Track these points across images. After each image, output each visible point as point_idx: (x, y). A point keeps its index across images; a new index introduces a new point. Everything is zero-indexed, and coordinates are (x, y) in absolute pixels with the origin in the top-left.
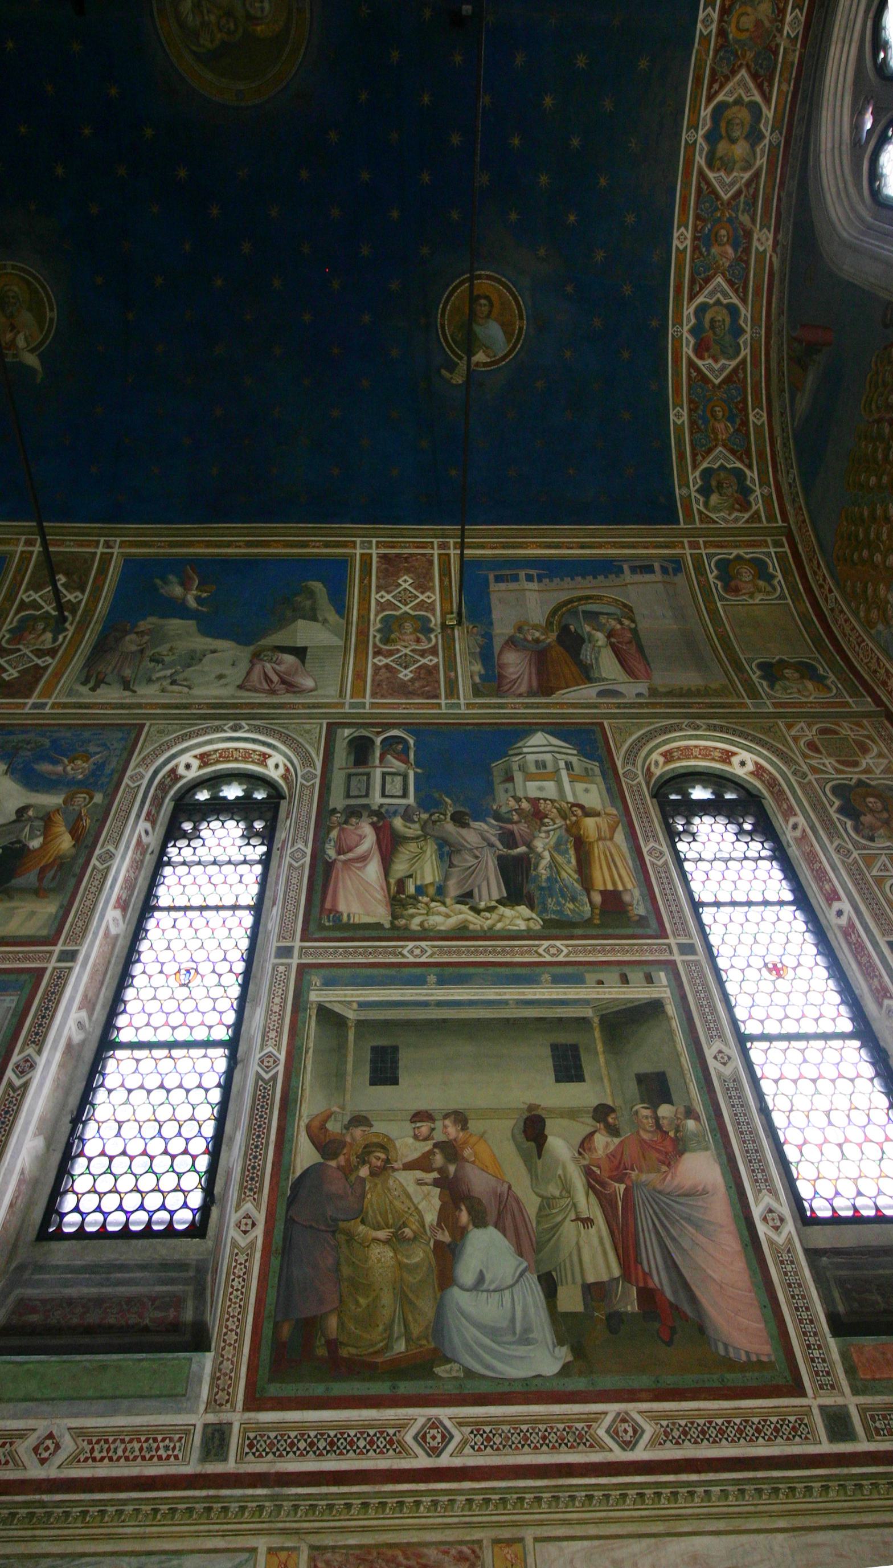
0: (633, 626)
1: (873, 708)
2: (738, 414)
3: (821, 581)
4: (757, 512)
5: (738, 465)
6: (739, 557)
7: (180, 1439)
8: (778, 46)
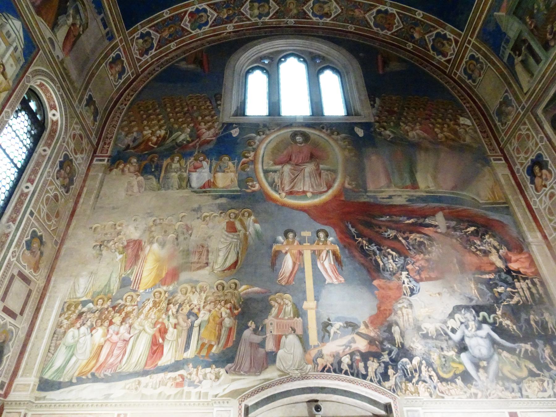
0: (81, 33)
1: (95, 143)
2: (173, 37)
3: (127, 99)
4: (141, 60)
5: (155, 45)
6: (123, 62)
8: (285, 18)
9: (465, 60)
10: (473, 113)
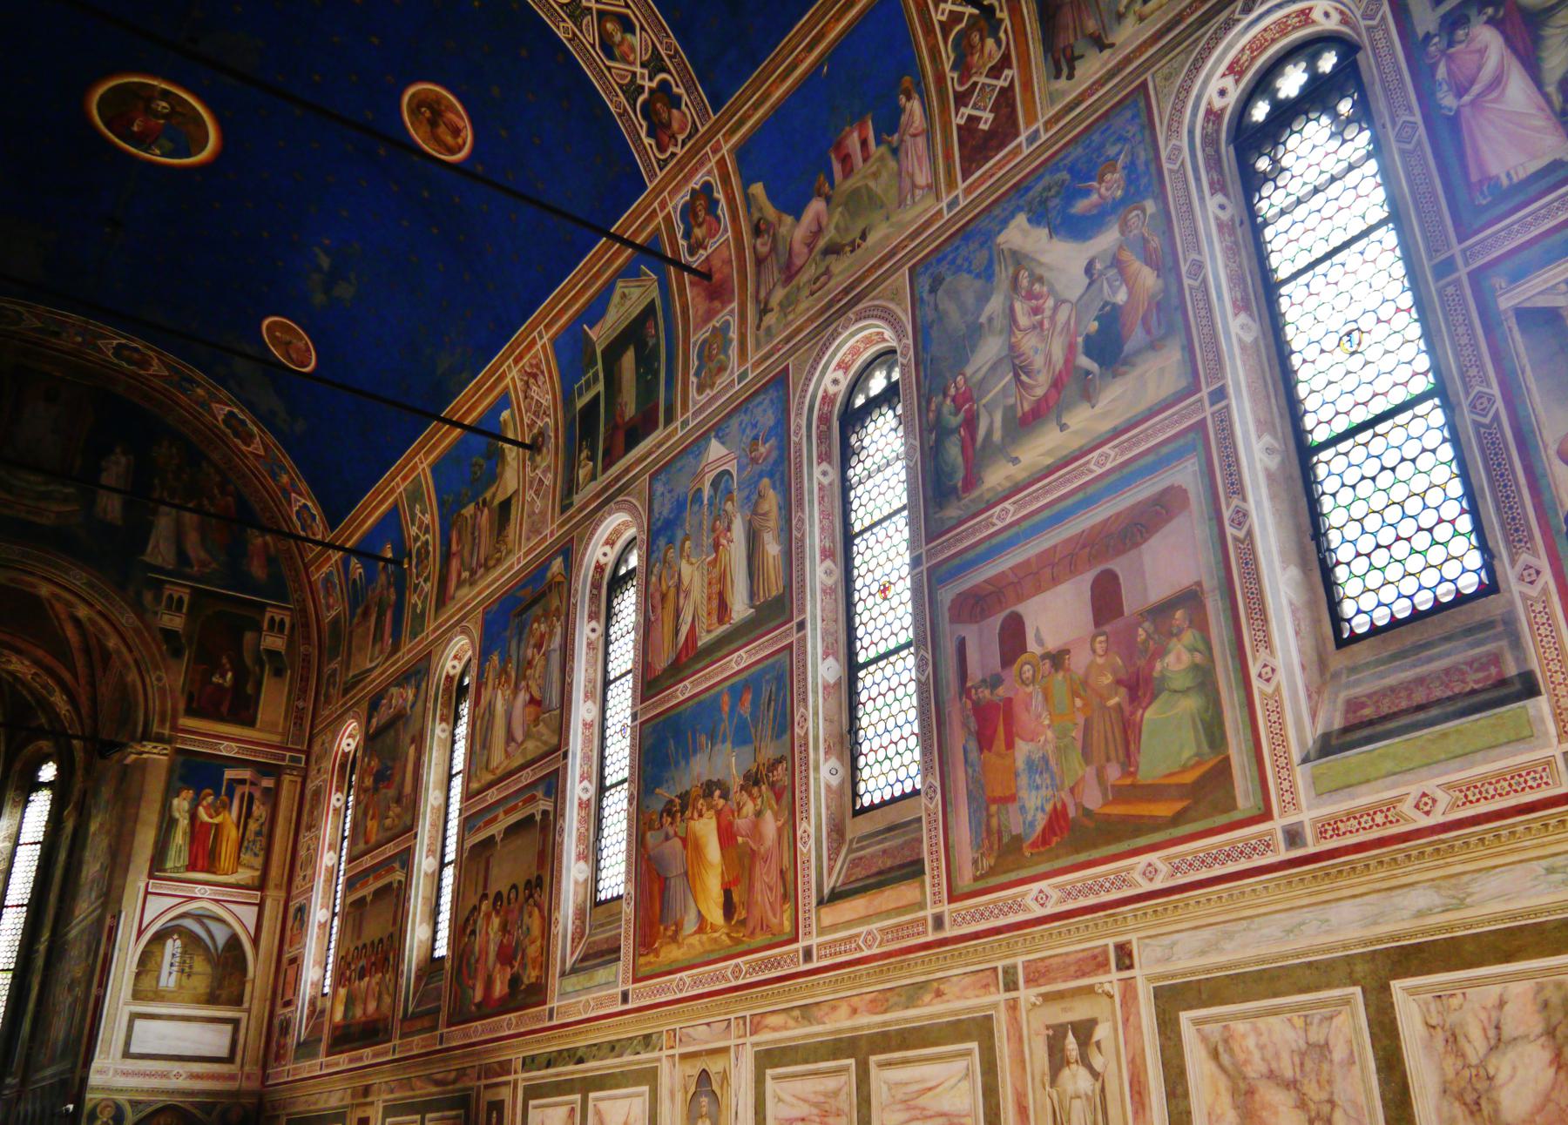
7: (1544, 769)
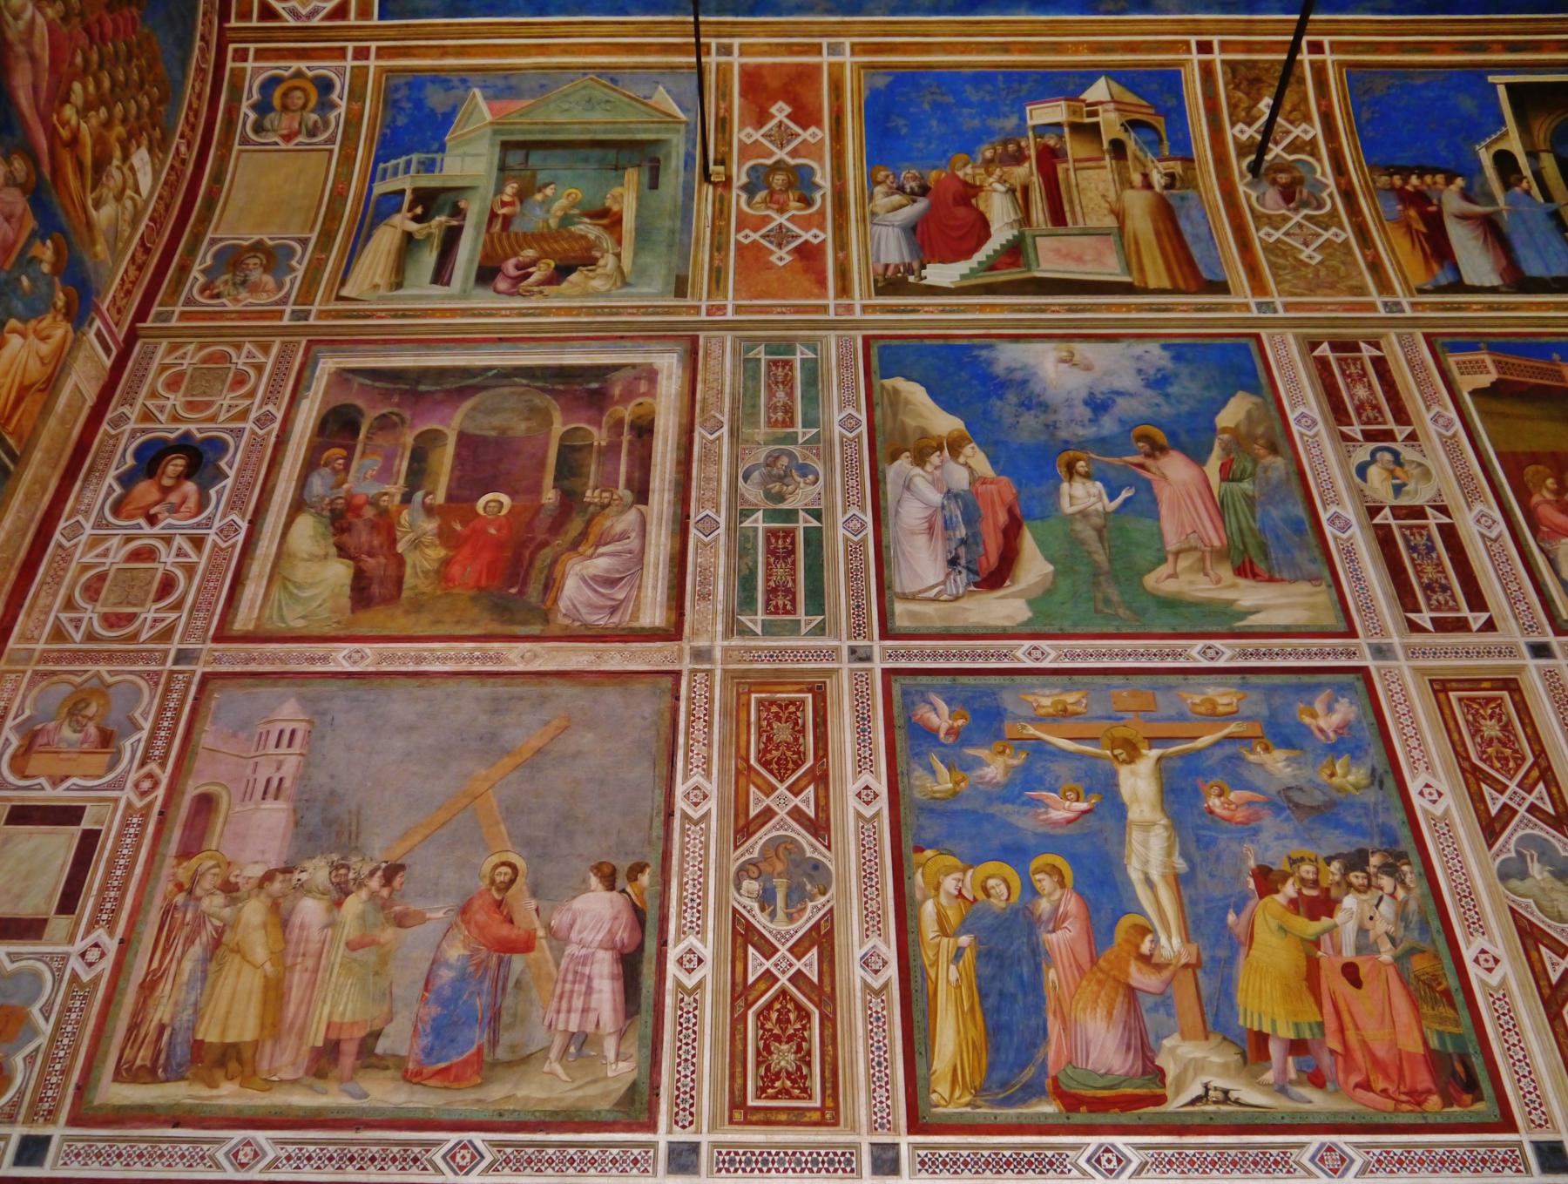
9: (302, 65)
10: (173, 177)
